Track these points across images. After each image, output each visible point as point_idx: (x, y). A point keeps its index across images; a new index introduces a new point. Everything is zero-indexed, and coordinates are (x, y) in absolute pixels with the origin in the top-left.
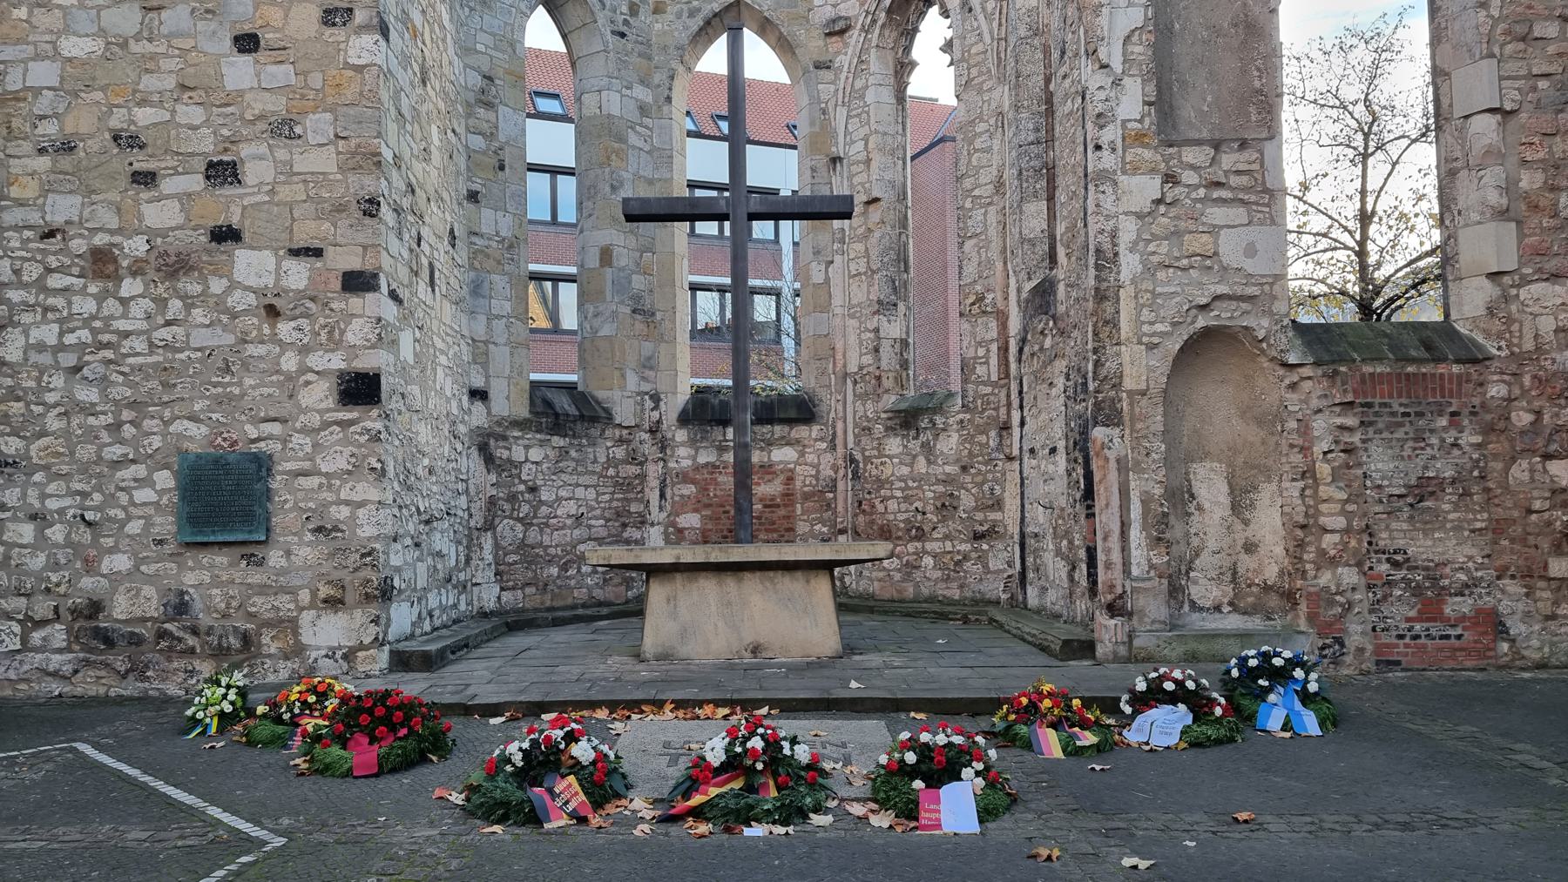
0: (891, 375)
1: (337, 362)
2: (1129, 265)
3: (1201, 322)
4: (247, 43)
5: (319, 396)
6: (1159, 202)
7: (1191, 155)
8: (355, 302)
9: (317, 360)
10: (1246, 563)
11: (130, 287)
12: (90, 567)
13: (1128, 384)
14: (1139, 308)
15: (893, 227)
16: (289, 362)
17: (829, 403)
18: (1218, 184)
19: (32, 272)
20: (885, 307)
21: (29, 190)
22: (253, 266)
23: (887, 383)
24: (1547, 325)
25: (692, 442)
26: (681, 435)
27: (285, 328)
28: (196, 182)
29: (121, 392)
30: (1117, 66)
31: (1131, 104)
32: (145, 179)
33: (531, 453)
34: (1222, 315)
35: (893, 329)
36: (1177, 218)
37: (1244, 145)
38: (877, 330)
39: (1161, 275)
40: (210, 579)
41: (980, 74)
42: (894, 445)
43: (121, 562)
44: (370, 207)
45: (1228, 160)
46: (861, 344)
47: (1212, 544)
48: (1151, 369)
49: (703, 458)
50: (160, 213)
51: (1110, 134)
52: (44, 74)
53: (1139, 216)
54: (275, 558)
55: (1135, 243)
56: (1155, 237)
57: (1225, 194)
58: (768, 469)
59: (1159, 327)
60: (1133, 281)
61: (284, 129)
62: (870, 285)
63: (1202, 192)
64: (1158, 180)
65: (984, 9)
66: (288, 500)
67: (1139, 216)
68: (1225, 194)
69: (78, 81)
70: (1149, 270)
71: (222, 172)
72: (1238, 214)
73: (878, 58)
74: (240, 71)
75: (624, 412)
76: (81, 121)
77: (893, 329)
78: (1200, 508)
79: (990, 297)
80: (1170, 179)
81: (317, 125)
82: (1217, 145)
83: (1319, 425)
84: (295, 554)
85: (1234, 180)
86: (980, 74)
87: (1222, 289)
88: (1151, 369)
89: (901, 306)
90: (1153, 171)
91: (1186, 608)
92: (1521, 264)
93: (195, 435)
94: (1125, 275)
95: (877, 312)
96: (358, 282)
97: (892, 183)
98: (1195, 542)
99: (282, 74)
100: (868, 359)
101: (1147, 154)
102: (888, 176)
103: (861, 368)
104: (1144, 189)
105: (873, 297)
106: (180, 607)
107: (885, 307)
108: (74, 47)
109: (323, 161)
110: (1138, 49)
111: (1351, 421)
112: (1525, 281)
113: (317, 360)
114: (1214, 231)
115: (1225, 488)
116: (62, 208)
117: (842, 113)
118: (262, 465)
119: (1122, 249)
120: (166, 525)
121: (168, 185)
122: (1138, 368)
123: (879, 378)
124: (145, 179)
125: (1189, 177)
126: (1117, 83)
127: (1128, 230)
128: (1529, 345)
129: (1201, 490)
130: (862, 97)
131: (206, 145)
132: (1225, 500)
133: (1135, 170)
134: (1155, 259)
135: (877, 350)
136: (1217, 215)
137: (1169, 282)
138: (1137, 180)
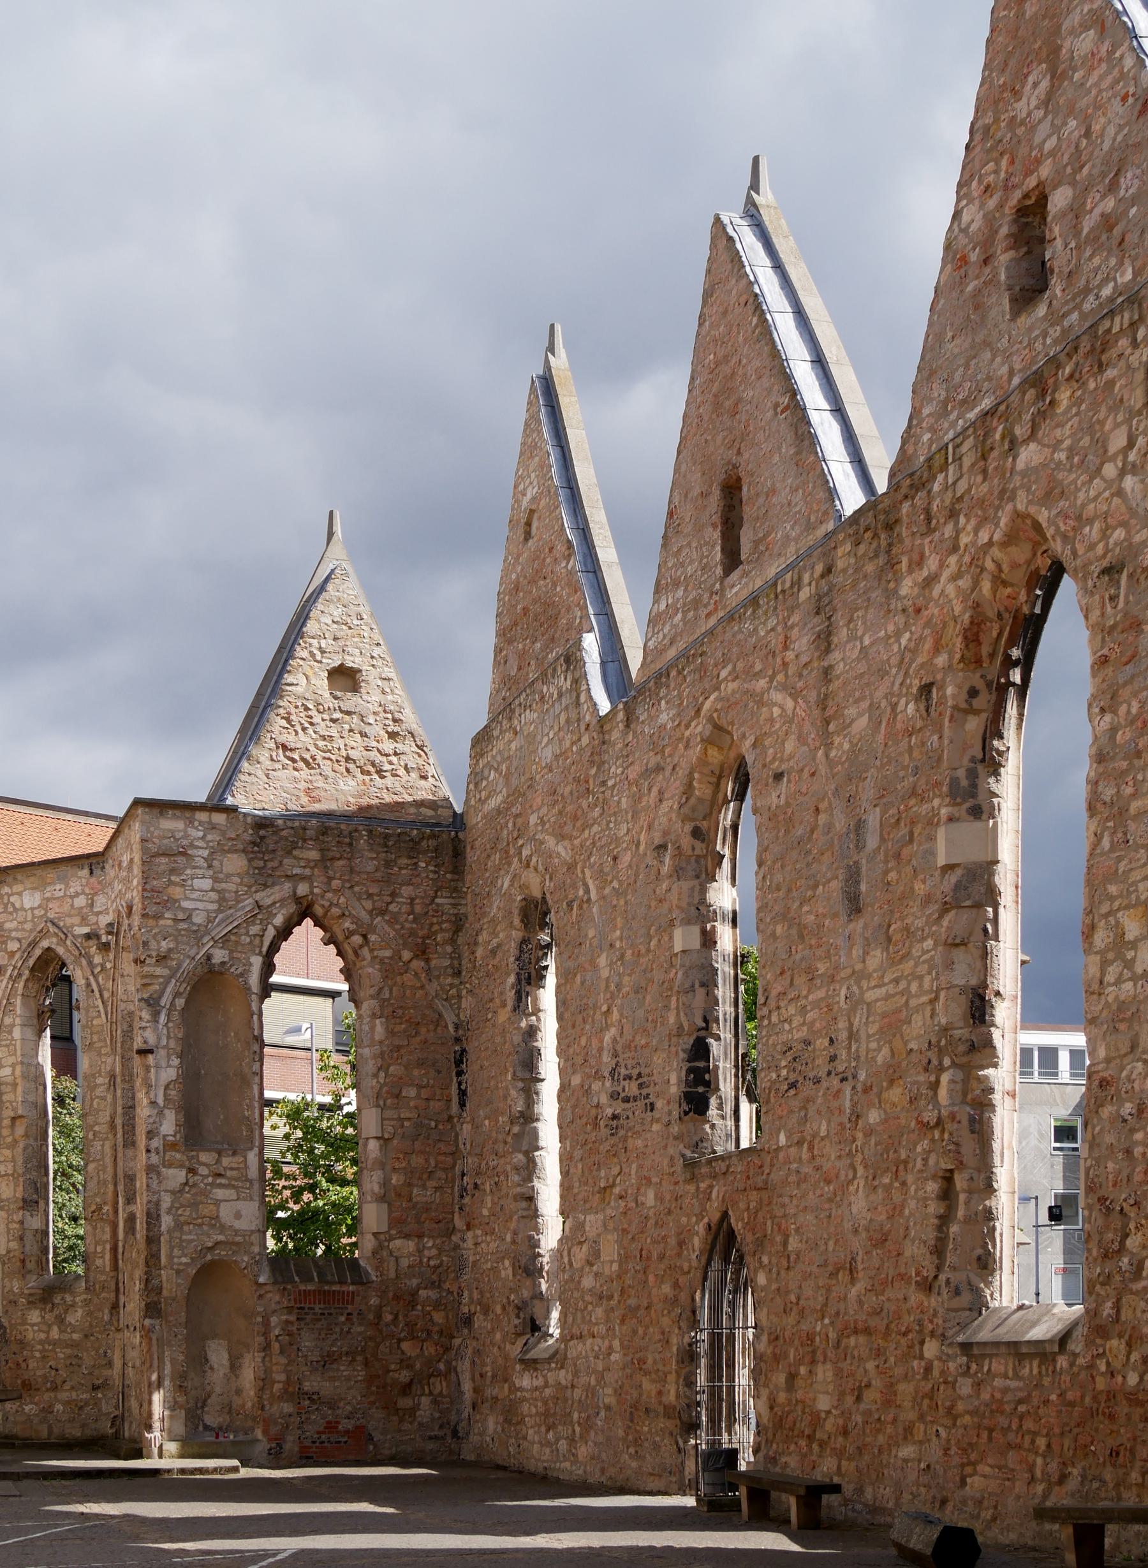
0: (33, 1259)
2: (166, 1221)
3: (209, 1257)
6: (186, 1184)
7: (204, 1157)
10: (237, 1401)
13: (165, 1293)
14: (172, 1248)
15: (36, 1140)
18: (220, 1175)
23: (30, 1265)
30: (160, 1101)
36: (195, 1194)
37: (234, 1153)
38: (22, 1222)
39: (186, 1228)
41: (100, 1040)
42: (34, 1316)
45: (226, 1161)
46: (9, 1230)
47: (218, 1390)
48: (178, 1285)
53: (173, 1192)
55: (170, 1209)
56: (182, 1206)
57: (223, 1181)
59: (184, 1260)
60: (169, 1231)
62: (16, 1185)
63: (210, 1179)
64: (184, 1172)
65: (101, 996)
67: (173, 1192)
68: (223, 1181)
70: (179, 1225)
72: (230, 1193)
73: (23, 1004)
78: (212, 1368)
79: (106, 1208)
80: (192, 1171)
82: (220, 1153)
83: (274, 1320)
85: (229, 1173)
86: (100, 1040)
87: (221, 1238)
88: (178, 1285)
89: (42, 1203)
90: (181, 1166)
91: (201, 1428)
92: (390, 1228)
94: (164, 1228)
95: (23, 1208)
97: (35, 1105)
98: (208, 1388)
100: (14, 1245)
101: (178, 1156)
102: (31, 1098)
103: (9, 1252)
104: (176, 1176)
105: (19, 1195)
110: (173, 1093)
111: (293, 1318)
112: (391, 1239)
114: (217, 1203)
115: (226, 1356)
119: (163, 1212)
122: (172, 1284)
123: (23, 1261)
125: (203, 1171)
126: (161, 1113)
127: (166, 1201)
128: (392, 1275)
129: (213, 1358)
130: (10, 1032)
132: (226, 1362)
133: (170, 1166)
134: (182, 1219)
135: (21, 1238)
136: (220, 1193)
137: (190, 1233)
138: (171, 1171)
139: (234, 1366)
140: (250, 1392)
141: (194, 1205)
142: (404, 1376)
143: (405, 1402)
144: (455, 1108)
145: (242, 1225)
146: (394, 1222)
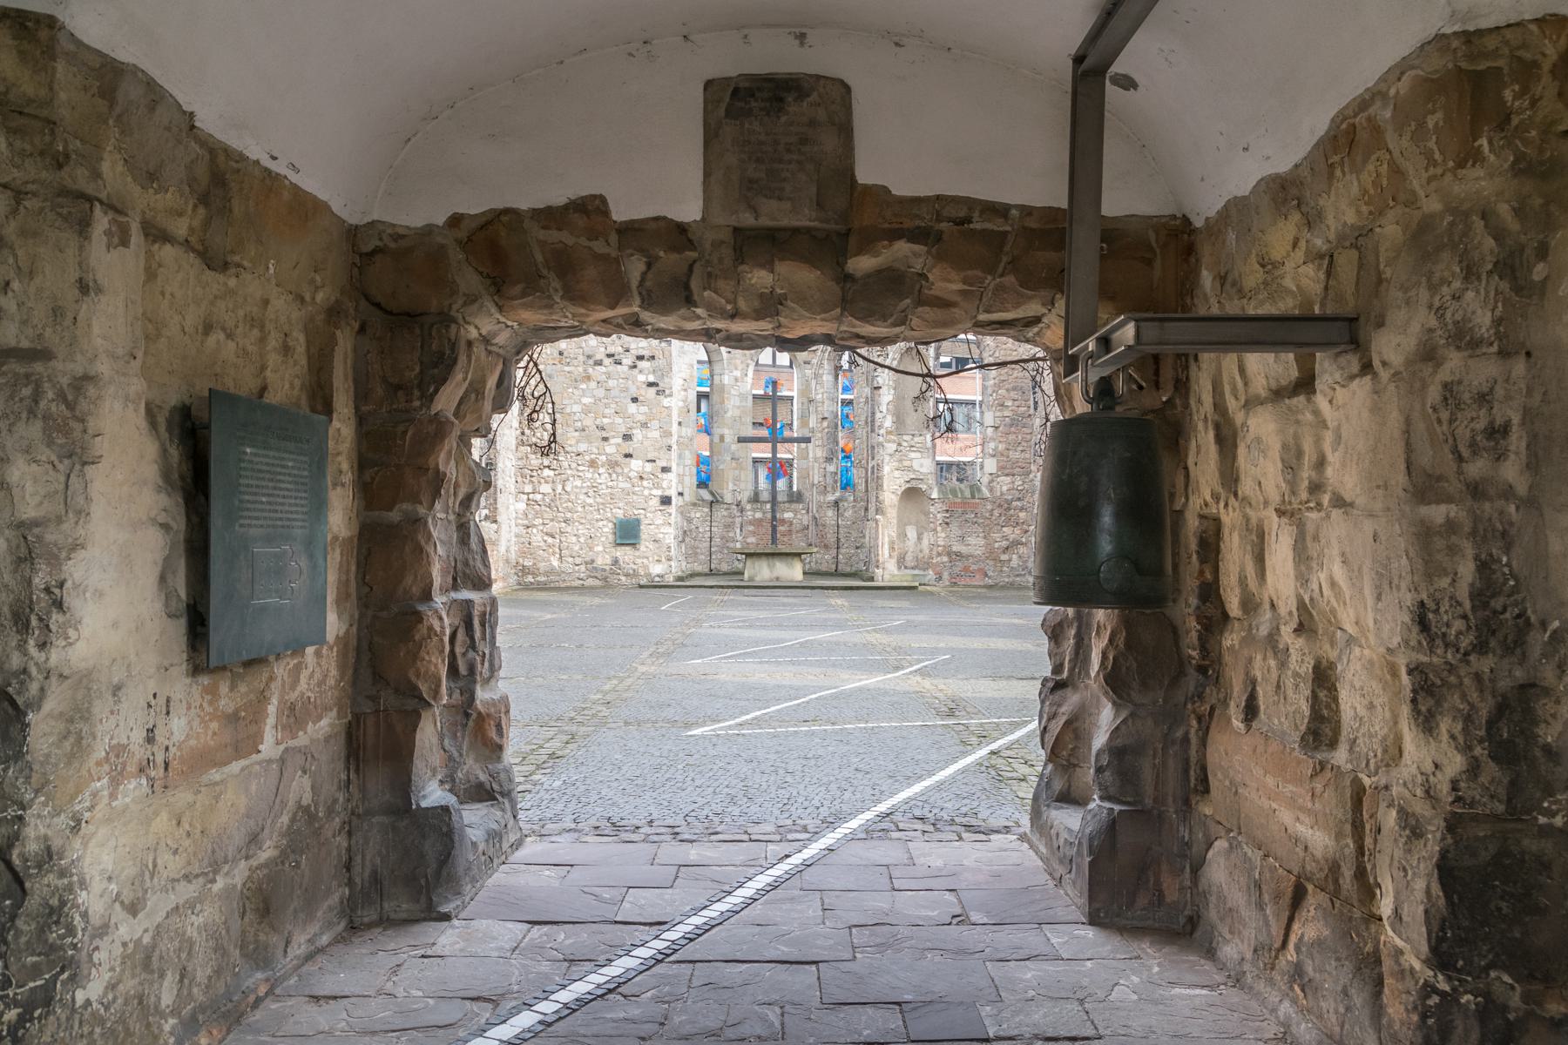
1: (659, 493)
4: (635, 400)
5: (655, 502)
8: (665, 476)
9: (655, 492)
11: (601, 470)
12: (591, 549)
16: (646, 492)
17: (807, 494)
19: (574, 465)
20: (829, 460)
21: (573, 442)
22: (636, 464)
24: (1005, 488)
25: (754, 510)
26: (749, 507)
27: (645, 483)
28: (620, 440)
29: (599, 500)
31: (888, 423)
32: (605, 439)
33: (697, 514)
34: (913, 484)
35: (831, 468)
40: (624, 554)
43: (600, 548)
44: (669, 448)
49: (758, 515)
50: (610, 449)
51: (882, 431)
52: (576, 408)
54: (642, 548)
58: (783, 521)
61: (644, 425)
66: (645, 531)
69: (587, 410)
71: (627, 437)
72: (918, 455)
74: (632, 408)
75: (728, 498)
76: (588, 422)
77: (831, 468)
81: (655, 424)
84: (645, 545)
93: (620, 514)
96: (665, 470)
99: (644, 409)
106: (616, 562)
107: (829, 460)
108: (586, 400)
109: (656, 434)
113: (655, 492)
116: (582, 447)
117: (813, 383)
118: (638, 521)
120: (611, 537)
121: (612, 441)
124: (605, 439)
127: (887, 458)
131: (623, 430)
136: (913, 455)
139: (919, 538)
140: (927, 551)
141: (900, 461)
142: (1005, 544)
143: (1004, 557)
144: (1032, 411)
145: (924, 470)
146: (1001, 468)
